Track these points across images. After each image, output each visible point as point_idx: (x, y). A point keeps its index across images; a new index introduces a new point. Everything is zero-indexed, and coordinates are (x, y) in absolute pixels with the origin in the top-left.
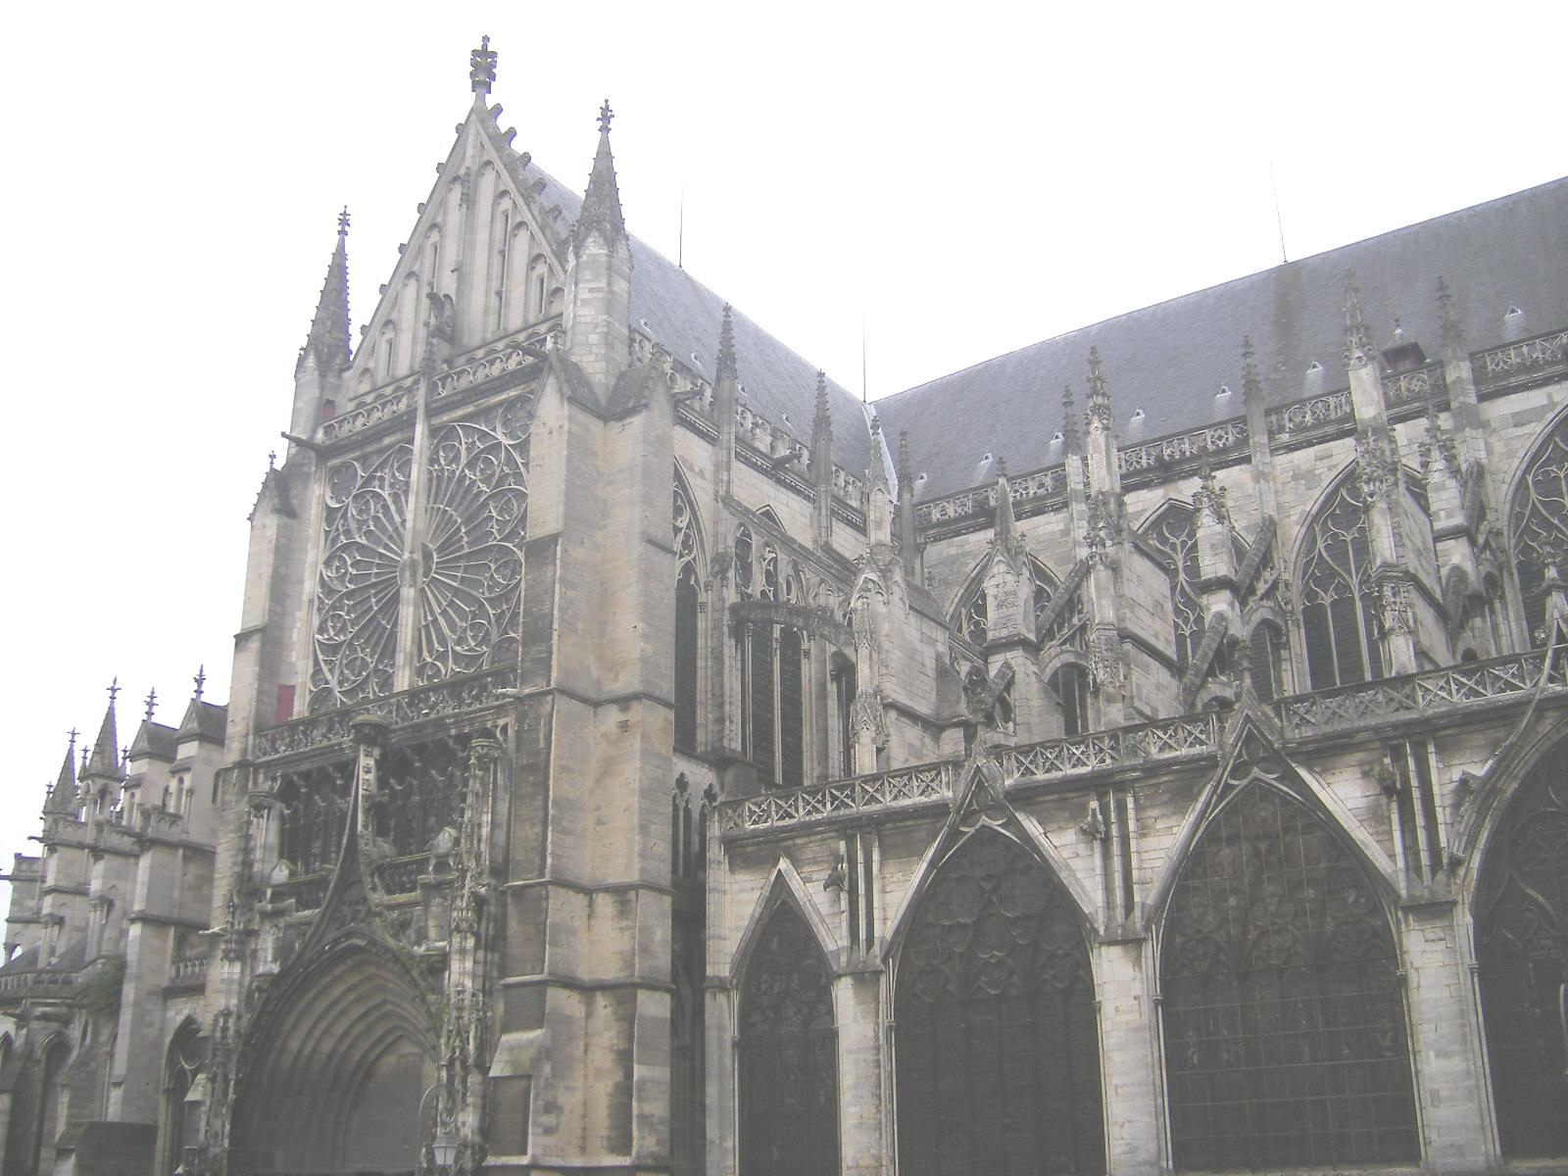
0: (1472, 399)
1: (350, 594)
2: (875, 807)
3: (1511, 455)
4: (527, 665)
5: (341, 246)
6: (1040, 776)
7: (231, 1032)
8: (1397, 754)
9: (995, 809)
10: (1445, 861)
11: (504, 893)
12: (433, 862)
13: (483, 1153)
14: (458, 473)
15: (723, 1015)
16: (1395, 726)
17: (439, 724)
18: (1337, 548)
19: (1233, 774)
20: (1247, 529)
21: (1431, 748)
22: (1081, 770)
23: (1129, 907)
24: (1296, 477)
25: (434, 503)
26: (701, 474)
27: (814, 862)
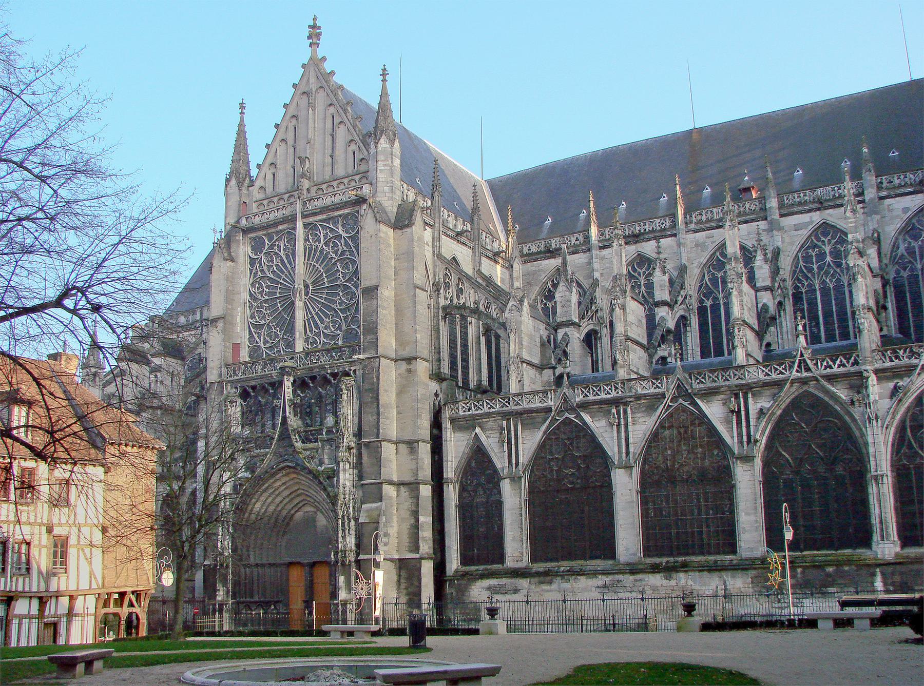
0: (777, 217)
1: (266, 301)
2: (519, 407)
3: (792, 244)
4: (366, 344)
5: (242, 120)
6: (591, 398)
8: (737, 396)
9: (572, 410)
10: (752, 440)
11: (361, 444)
12: (325, 430)
13: (358, 555)
14: (320, 247)
15: (451, 494)
16: (736, 386)
17: (323, 367)
18: (714, 280)
19: (671, 402)
20: (673, 268)
21: (750, 395)
22: (609, 396)
23: (628, 453)
24: (697, 245)
25: (308, 260)
26: (427, 244)
27: (491, 429)
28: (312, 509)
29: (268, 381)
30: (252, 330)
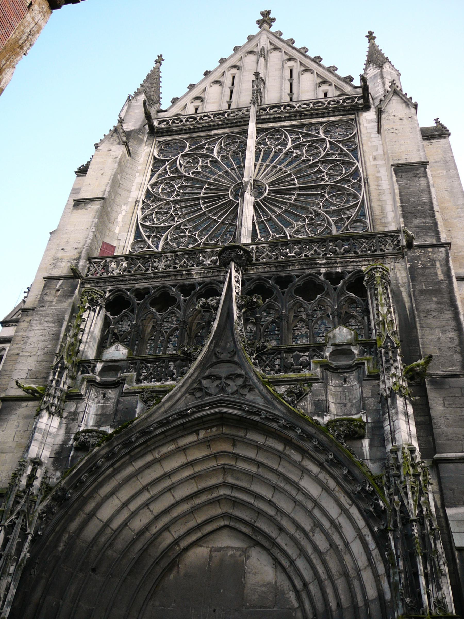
7: (37, 483)
29: (180, 283)
30: (143, 234)
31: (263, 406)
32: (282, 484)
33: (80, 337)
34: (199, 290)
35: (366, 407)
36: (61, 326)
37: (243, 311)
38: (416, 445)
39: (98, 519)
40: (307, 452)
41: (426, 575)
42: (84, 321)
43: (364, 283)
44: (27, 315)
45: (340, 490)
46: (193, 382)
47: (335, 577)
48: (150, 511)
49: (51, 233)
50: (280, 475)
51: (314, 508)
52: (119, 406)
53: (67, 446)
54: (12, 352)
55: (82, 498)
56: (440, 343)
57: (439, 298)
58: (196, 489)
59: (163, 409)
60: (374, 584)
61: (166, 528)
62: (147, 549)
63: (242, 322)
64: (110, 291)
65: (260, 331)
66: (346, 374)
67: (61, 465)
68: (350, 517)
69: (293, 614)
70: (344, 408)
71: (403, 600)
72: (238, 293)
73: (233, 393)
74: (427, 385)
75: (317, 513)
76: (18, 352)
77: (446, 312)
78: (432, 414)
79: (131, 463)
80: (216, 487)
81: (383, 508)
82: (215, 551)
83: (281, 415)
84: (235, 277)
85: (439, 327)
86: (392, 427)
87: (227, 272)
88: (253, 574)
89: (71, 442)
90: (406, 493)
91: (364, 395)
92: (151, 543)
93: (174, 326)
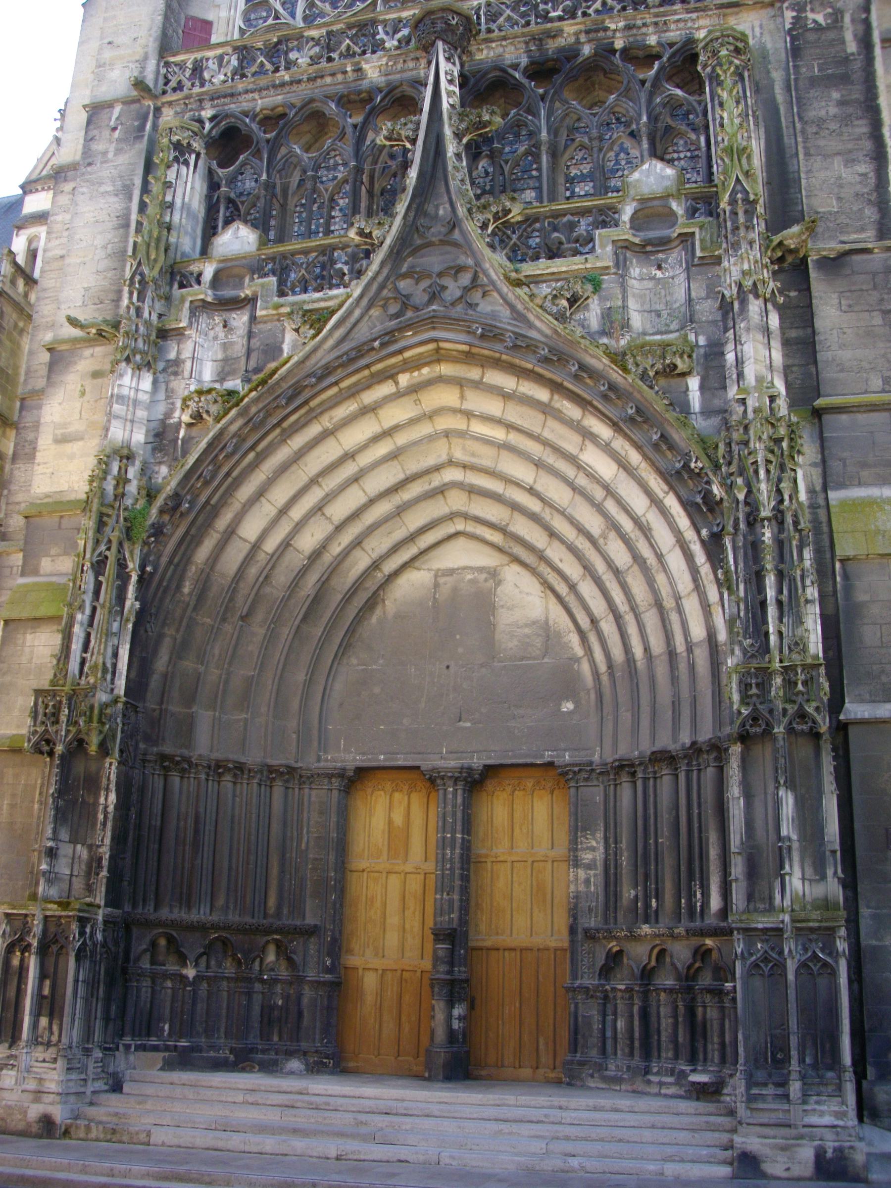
28: (485, 558)
31: (509, 324)
32: (551, 459)
33: (167, 219)
34: (381, 101)
35: (696, 317)
36: (130, 199)
37: (465, 141)
38: (780, 386)
39: (240, 538)
40: (590, 404)
41: (780, 603)
42: (169, 187)
43: (699, 68)
44: (66, 180)
45: (649, 468)
46: (382, 287)
47: (642, 609)
48: (327, 518)
49: (84, 5)
50: (545, 443)
51: (605, 499)
52: (253, 341)
53: (172, 421)
54: (49, 254)
55: (208, 507)
56: (841, 186)
57: (844, 92)
58: (401, 476)
59: (330, 342)
60: (701, 619)
61: (357, 543)
62: (328, 579)
63: (464, 163)
64: (212, 119)
65: (503, 174)
66: (661, 256)
67: (165, 455)
68: (664, 512)
69: (576, 666)
70: (657, 320)
71: (740, 643)
72: (452, 106)
73: (453, 304)
74: (811, 271)
75: (610, 506)
76: (59, 252)
77: (856, 123)
78: (816, 325)
79: (285, 441)
80: (437, 468)
81: (718, 498)
82: (443, 575)
83: (543, 339)
84: (446, 73)
85: (838, 154)
86: (739, 354)
87: (429, 63)
88: (508, 609)
89: (177, 414)
90: (756, 472)
91: (693, 294)
92: (334, 569)
93: (340, 176)
